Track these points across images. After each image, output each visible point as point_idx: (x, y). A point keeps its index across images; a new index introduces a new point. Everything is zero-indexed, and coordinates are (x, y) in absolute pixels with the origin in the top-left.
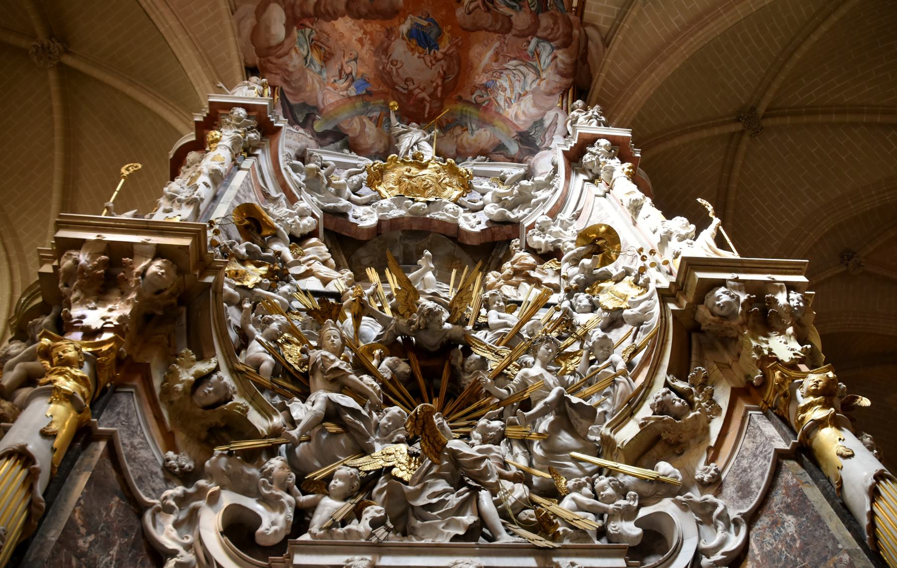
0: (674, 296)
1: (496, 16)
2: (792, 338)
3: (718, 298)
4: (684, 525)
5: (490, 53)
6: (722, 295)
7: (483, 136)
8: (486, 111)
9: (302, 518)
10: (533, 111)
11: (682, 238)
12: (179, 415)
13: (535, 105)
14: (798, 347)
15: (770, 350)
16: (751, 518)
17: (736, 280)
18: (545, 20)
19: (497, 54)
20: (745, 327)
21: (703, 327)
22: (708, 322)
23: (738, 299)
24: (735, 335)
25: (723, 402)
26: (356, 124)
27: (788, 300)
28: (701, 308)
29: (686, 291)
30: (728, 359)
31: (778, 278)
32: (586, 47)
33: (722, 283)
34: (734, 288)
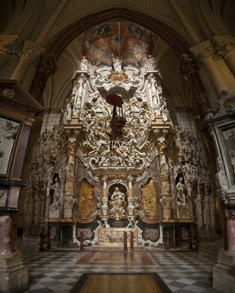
1: (133, 35)
4: (144, 162)
5: (132, 43)
7: (131, 60)
8: (132, 56)
9: (100, 160)
10: (141, 57)
12: (84, 149)
13: (141, 55)
16: (151, 162)
18: (143, 37)
19: (133, 43)
25: (153, 145)
26: (105, 60)
32: (152, 42)
33: (156, 129)
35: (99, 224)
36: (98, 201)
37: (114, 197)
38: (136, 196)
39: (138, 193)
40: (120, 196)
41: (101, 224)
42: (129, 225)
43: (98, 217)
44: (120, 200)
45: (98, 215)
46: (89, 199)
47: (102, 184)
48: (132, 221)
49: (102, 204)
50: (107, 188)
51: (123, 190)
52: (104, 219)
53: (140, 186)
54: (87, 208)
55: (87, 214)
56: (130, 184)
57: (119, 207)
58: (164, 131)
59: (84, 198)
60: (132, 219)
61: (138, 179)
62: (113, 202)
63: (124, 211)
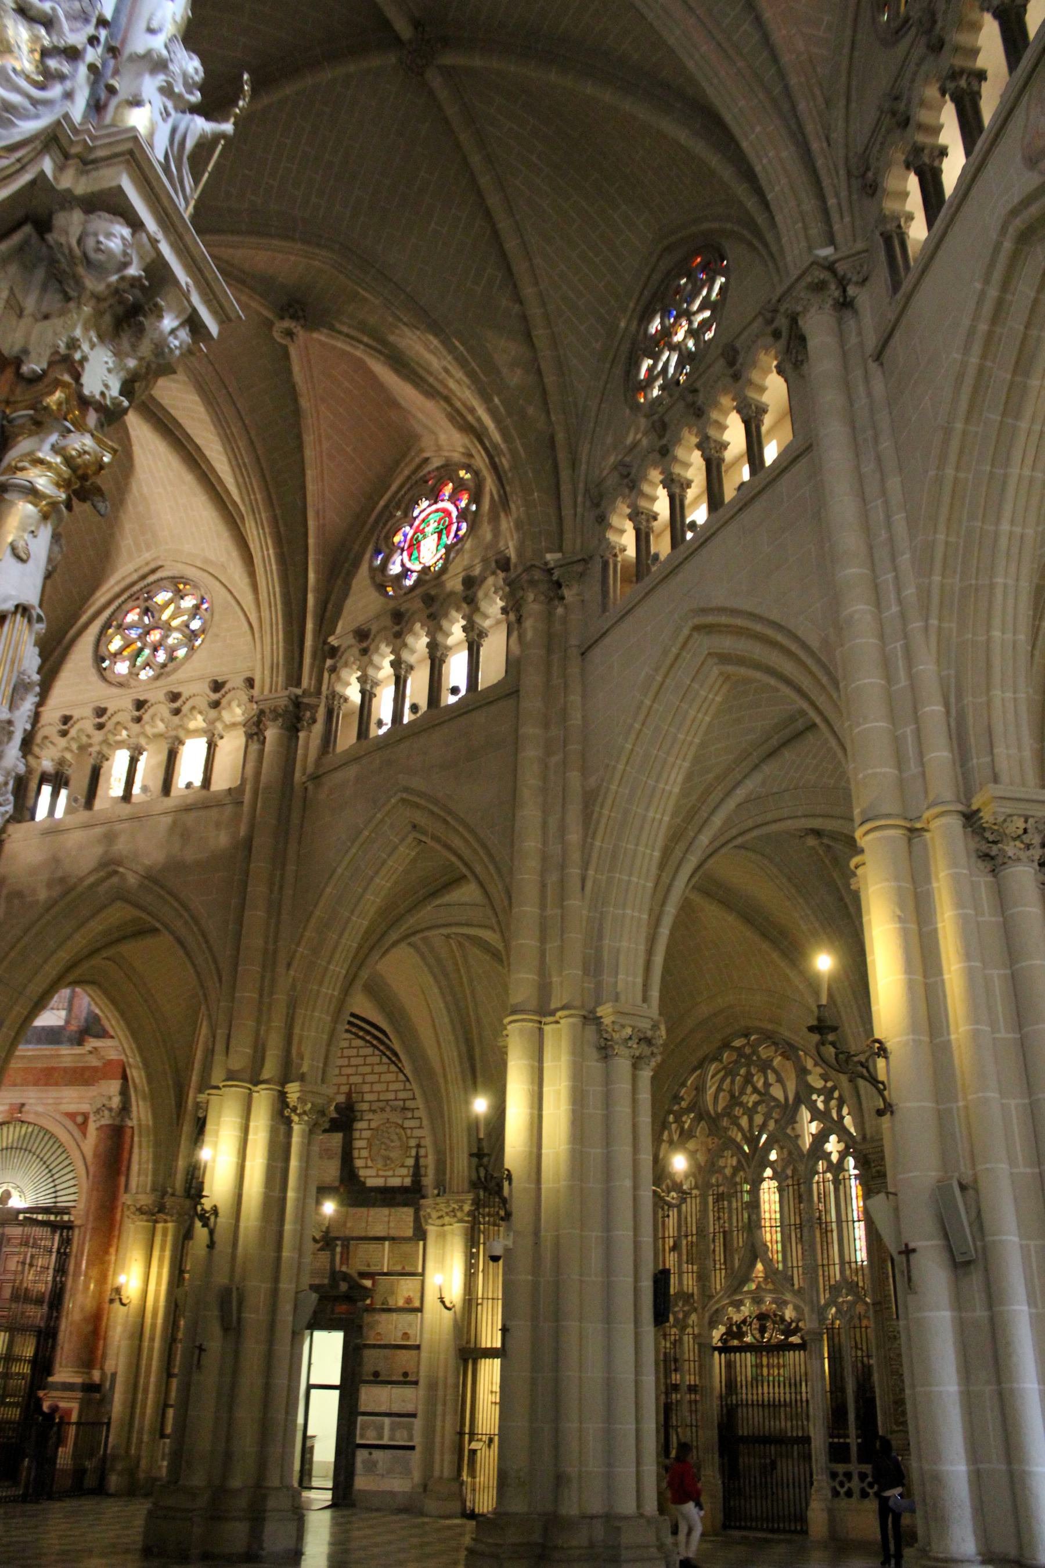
0: (67, 156)
2: (123, 374)
3: (109, 235)
6: (116, 237)
11: (167, 91)
14: (115, 391)
15: (85, 358)
17: (154, 242)
20: (93, 303)
21: (49, 237)
22: (63, 240)
23: (126, 265)
24: (73, 294)
27: (173, 332)
28: (77, 216)
29: (87, 172)
30: (30, 303)
31: (196, 299)
33: (136, 224)
34: (139, 246)
58: (168, 322)
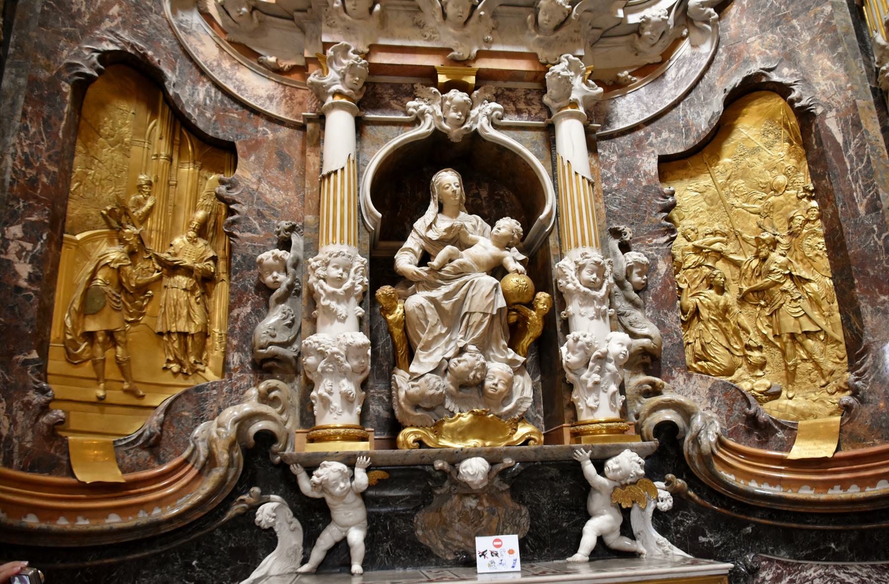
35: (268, 540)
36: (265, 290)
37: (425, 259)
38: (625, 247)
39: (637, 220)
40: (484, 247)
41: (290, 536)
42: (588, 540)
43: (261, 461)
44: (487, 281)
45: (266, 438)
46: (173, 269)
47: (312, 129)
48: (623, 485)
49: (311, 309)
50: (359, 166)
51: (502, 185)
52: (330, 471)
53: (650, 165)
54: (152, 361)
55: (136, 426)
56: (571, 135)
57: (484, 345)
59: (114, 253)
60: (628, 462)
61: (629, 109)
62: (418, 299)
63: (525, 388)
